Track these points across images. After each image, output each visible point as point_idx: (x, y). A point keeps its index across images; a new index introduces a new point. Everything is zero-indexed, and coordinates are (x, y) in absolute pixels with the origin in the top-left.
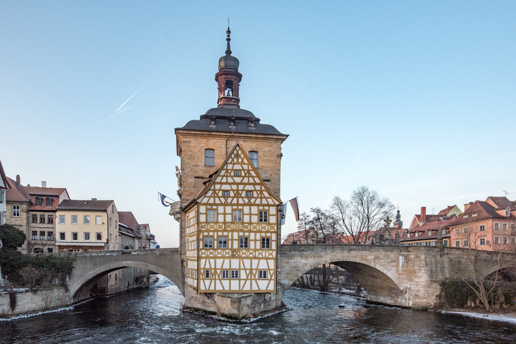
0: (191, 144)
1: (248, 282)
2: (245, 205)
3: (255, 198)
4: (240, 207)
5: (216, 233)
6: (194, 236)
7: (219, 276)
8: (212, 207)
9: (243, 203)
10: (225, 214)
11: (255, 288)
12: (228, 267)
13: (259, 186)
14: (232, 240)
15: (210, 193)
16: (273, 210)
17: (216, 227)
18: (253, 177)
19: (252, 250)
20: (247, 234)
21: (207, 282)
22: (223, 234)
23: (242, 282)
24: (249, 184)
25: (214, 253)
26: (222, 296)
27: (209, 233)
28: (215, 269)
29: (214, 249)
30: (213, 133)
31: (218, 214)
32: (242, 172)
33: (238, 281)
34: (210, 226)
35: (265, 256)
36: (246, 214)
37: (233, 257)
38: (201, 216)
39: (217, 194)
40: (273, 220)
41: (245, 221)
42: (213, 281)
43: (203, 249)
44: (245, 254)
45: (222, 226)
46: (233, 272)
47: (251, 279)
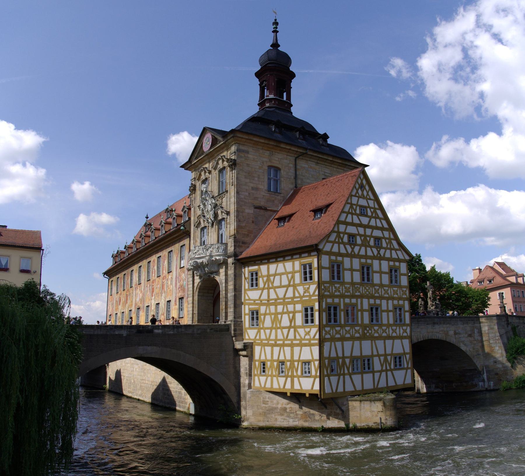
0: (249, 156)
2: (373, 258)
3: (384, 248)
4: (369, 261)
5: (342, 300)
6: (294, 303)
8: (336, 258)
9: (372, 255)
10: (352, 270)
13: (387, 232)
14: (362, 311)
16: (403, 268)
17: (342, 290)
18: (380, 219)
19: (385, 325)
20: (378, 302)
21: (334, 379)
22: (351, 301)
24: (377, 228)
25: (341, 332)
27: (333, 300)
28: (344, 358)
29: (340, 326)
31: (344, 269)
32: (368, 209)
34: (335, 287)
36: (376, 272)
38: (323, 271)
39: (342, 239)
40: (404, 281)
42: (342, 377)
43: (327, 326)
45: (349, 288)
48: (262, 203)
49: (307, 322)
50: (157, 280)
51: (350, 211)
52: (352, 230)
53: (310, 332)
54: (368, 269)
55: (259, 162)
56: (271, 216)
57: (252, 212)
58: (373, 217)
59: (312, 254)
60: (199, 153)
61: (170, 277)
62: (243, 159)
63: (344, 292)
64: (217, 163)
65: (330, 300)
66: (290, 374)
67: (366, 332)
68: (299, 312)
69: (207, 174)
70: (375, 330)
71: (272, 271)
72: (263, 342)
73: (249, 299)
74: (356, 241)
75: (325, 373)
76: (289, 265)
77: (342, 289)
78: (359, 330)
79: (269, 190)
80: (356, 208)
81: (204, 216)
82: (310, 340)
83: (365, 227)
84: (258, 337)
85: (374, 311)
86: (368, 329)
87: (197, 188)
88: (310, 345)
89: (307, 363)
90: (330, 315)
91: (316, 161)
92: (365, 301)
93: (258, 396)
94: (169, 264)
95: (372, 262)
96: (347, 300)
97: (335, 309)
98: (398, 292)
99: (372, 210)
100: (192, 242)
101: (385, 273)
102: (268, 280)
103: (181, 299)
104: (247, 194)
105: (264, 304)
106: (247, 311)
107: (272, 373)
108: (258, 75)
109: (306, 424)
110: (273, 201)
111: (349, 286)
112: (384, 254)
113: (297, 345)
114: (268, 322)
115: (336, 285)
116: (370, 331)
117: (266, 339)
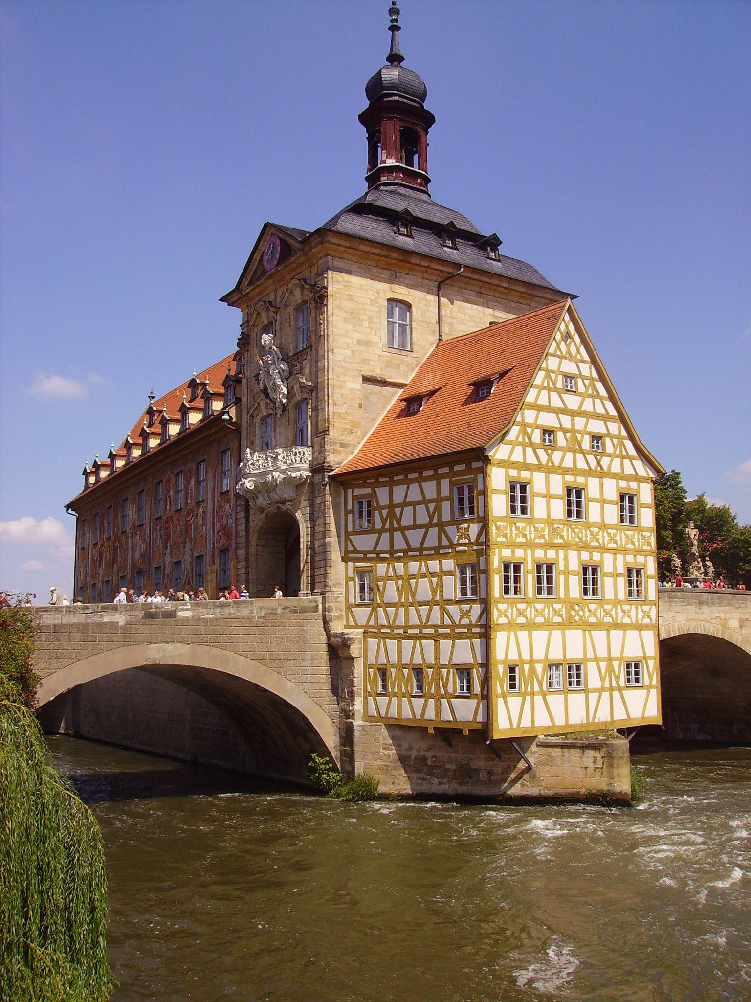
1: (606, 695)
2: (589, 473)
4: (581, 480)
5: (529, 552)
7: (540, 684)
11: (620, 715)
12: (562, 657)
14: (567, 573)
15: (514, 431)
16: (646, 494)
19: (609, 602)
20: (596, 557)
21: (514, 702)
22: (545, 554)
23: (593, 697)
24: (596, 416)
25: (528, 613)
26: (563, 746)
27: (513, 552)
28: (532, 662)
29: (525, 600)
30: (414, 260)
32: (579, 380)
33: (582, 696)
34: (517, 529)
35: (637, 619)
36: (594, 500)
37: (568, 624)
39: (530, 438)
40: (647, 518)
41: (591, 520)
42: (528, 698)
44: (595, 616)
45: (543, 530)
46: (570, 669)
47: (611, 689)
48: (377, 372)
49: (464, 592)
50: (174, 518)
51: (546, 384)
52: (548, 420)
53: (469, 611)
54: (579, 495)
55: (370, 292)
56: (394, 395)
57: (359, 387)
58: (589, 396)
59: (475, 465)
60: (255, 273)
61: (201, 511)
62: (341, 286)
63: (533, 536)
64: (292, 293)
65: (507, 553)
66: (433, 691)
67: (573, 613)
68: (450, 573)
69: (271, 314)
70: (590, 611)
71: (398, 498)
72: (383, 631)
73: (356, 551)
74: (555, 442)
75: (499, 691)
76: (430, 489)
77: (530, 531)
78: (561, 610)
79: (390, 345)
80: (556, 377)
81: (267, 395)
82: (469, 626)
83: (573, 414)
84: (372, 623)
85: (590, 575)
86: (577, 607)
87: (253, 341)
88: (470, 636)
89: (464, 672)
90: (506, 580)
91: (478, 289)
92: (573, 555)
93: (374, 736)
94: (198, 483)
95: (587, 481)
96: (539, 554)
97: (517, 568)
98: (636, 540)
99: (587, 382)
100: (244, 443)
101: (611, 502)
102: (391, 514)
103: (224, 551)
104: (349, 353)
105: (383, 560)
106: (351, 573)
107: (400, 688)
108: (364, 118)
109: (463, 790)
110: (399, 365)
111: (542, 525)
112: (609, 466)
113: (446, 636)
114: (391, 592)
115: (518, 524)
116: (581, 613)
117: (389, 627)
